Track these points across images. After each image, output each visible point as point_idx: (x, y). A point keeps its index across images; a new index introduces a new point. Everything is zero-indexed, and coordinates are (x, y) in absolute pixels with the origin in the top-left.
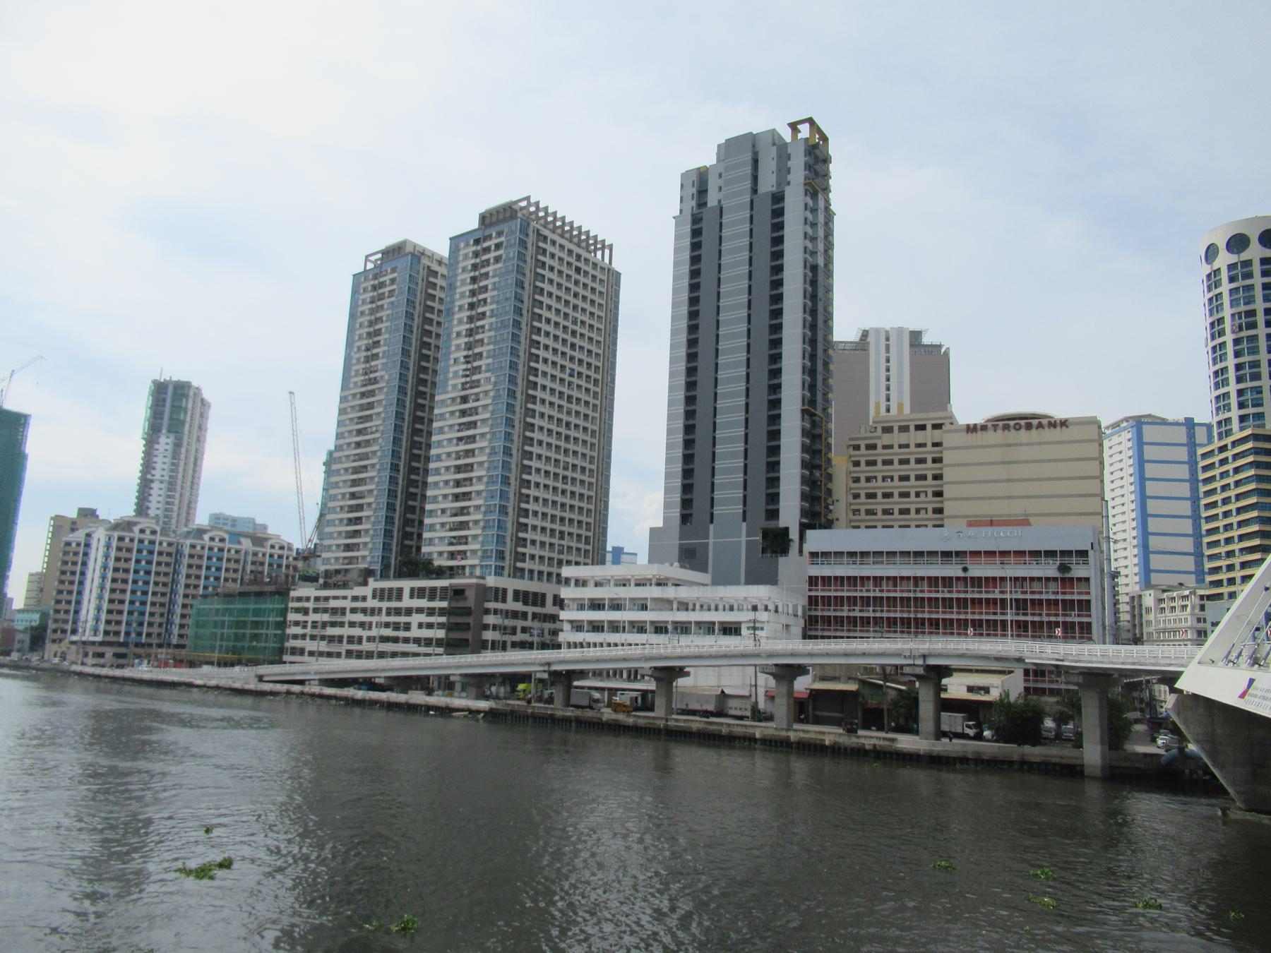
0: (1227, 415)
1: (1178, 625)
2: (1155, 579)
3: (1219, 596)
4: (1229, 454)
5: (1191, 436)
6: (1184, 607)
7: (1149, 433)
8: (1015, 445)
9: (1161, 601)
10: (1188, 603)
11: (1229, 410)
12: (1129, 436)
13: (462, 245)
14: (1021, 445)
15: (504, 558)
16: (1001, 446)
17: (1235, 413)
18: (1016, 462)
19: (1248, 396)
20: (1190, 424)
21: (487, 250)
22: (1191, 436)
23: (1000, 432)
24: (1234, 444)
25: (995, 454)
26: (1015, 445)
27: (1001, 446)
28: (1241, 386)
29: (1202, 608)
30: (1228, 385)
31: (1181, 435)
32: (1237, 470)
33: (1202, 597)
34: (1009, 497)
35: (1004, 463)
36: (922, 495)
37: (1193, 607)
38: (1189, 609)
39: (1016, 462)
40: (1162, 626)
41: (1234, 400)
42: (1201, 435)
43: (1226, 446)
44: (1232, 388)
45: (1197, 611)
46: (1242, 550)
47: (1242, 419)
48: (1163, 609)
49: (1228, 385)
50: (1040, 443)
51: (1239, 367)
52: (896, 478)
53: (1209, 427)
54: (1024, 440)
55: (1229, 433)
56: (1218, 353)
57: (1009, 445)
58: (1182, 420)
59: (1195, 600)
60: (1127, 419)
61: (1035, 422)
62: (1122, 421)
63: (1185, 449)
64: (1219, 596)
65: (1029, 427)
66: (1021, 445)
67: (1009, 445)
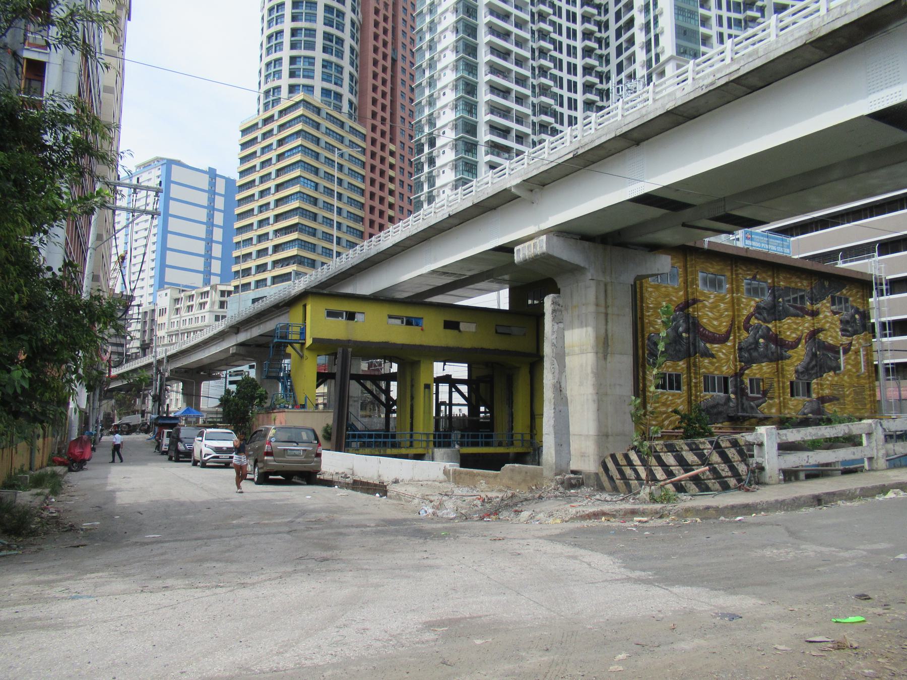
0: (277, 83)
1: (194, 325)
2: (171, 276)
3: (246, 286)
4: (274, 126)
5: (212, 184)
6: (202, 305)
7: (177, 174)
9: (177, 300)
10: (208, 300)
11: (280, 78)
12: (159, 173)
17: (285, 81)
19: (301, 65)
20: (212, 174)
22: (212, 184)
24: (282, 113)
28: (295, 53)
29: (222, 305)
30: (281, 50)
31: (204, 182)
32: (281, 142)
33: (223, 293)
37: (213, 303)
38: (207, 307)
40: (176, 328)
41: (286, 67)
42: (220, 187)
43: (272, 117)
44: (286, 53)
45: (216, 307)
46: (276, 231)
47: (292, 89)
48: (177, 310)
49: (281, 50)
51: (294, 32)
53: (229, 182)
55: (277, 101)
56: (275, 14)
58: (206, 168)
59: (216, 297)
60: (158, 160)
62: (153, 161)
63: (206, 195)
64: (246, 286)
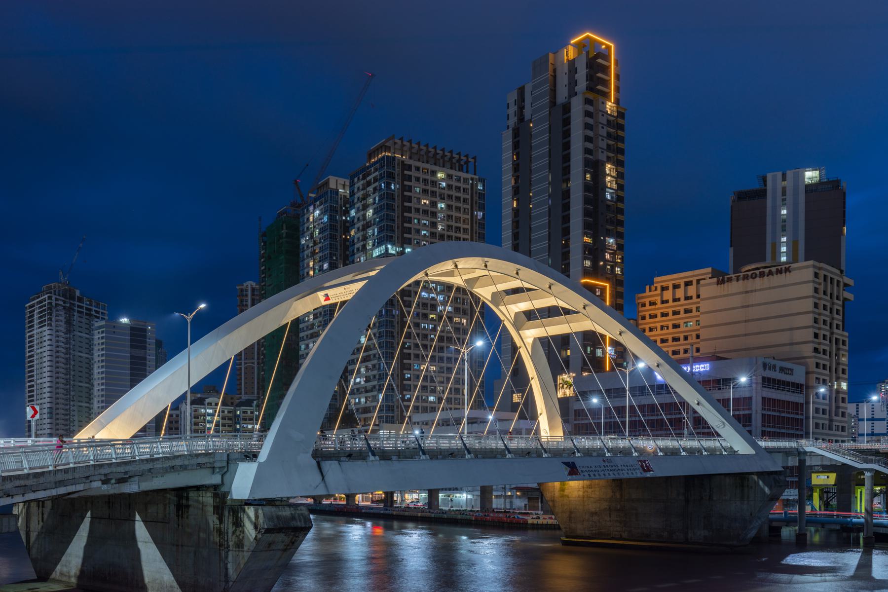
8: (752, 291)
13: (356, 179)
14: (755, 291)
15: (393, 410)
16: (742, 293)
18: (752, 306)
21: (369, 184)
23: (741, 282)
25: (736, 301)
26: (752, 291)
27: (742, 293)
34: (746, 335)
35: (743, 307)
36: (689, 338)
39: (752, 306)
50: (770, 288)
52: (670, 327)
54: (758, 287)
57: (747, 292)
61: (774, 269)
65: (762, 275)
66: (755, 291)
67: (747, 292)
